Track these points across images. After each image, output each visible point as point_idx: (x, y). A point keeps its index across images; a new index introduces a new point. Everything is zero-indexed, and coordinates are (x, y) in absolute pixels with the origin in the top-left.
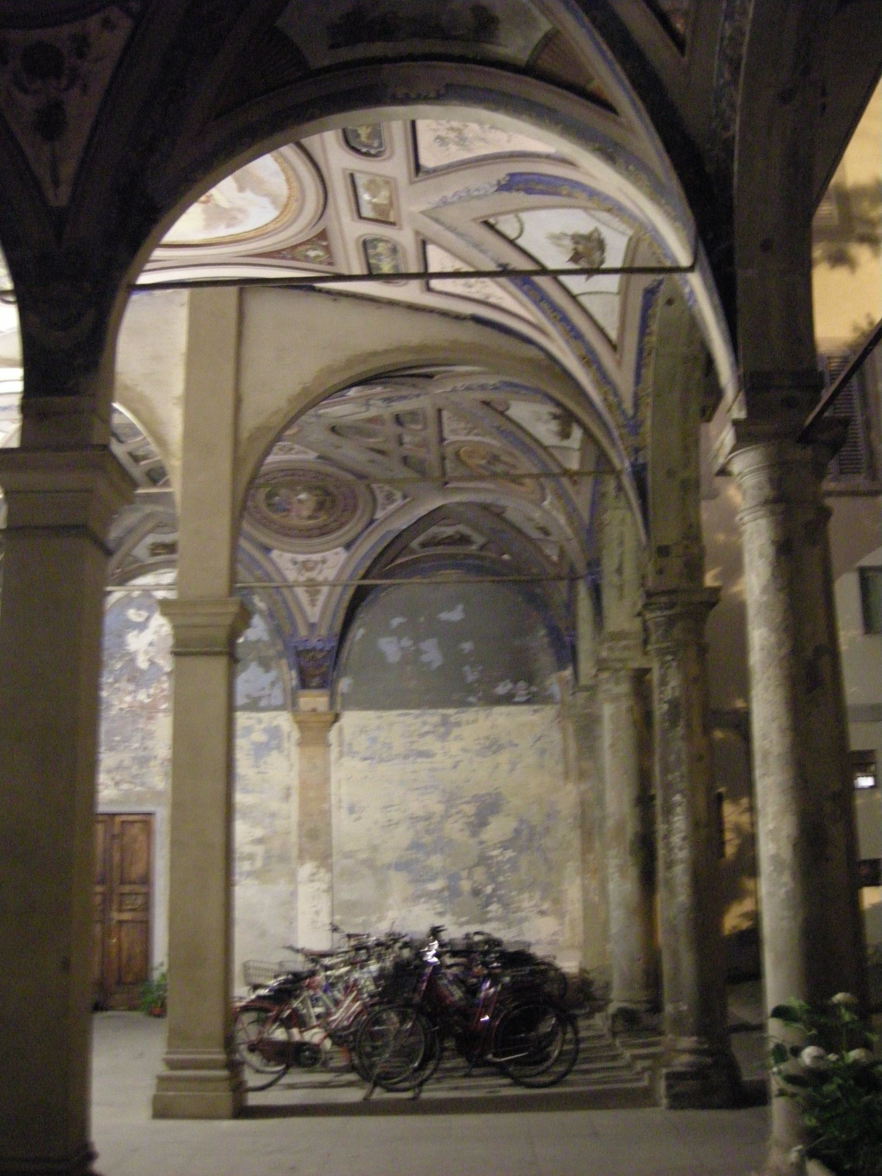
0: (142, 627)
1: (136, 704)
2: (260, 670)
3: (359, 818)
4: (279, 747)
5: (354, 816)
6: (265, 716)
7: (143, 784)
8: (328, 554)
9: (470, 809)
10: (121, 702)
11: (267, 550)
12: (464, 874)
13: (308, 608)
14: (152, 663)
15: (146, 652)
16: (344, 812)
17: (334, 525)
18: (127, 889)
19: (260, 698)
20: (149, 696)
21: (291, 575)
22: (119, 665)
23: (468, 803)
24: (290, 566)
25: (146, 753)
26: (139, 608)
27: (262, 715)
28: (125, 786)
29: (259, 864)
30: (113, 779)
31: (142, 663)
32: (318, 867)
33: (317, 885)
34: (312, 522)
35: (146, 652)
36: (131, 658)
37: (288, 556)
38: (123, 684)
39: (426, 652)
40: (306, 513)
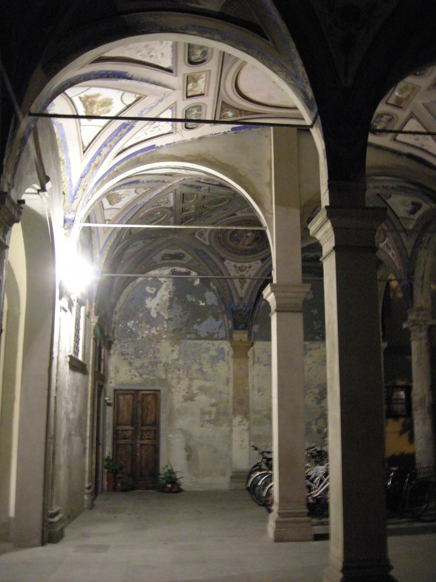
0: (154, 296)
1: (151, 335)
2: (214, 320)
3: (263, 395)
4: (223, 359)
5: (260, 394)
6: (217, 343)
7: (154, 375)
8: (253, 264)
9: (316, 391)
10: (143, 333)
11: (223, 260)
12: (314, 422)
13: (239, 290)
14: (158, 313)
15: (155, 309)
16: (256, 391)
18: (145, 428)
19: (214, 334)
20: (157, 331)
21: (233, 273)
22: (141, 315)
23: (316, 388)
24: (233, 268)
25: (156, 360)
26: (151, 286)
27: (215, 342)
28: (145, 376)
29: (213, 416)
30: (138, 373)
31: (154, 314)
32: (243, 418)
33: (242, 427)
34: (248, 247)
35: (155, 309)
36: (149, 312)
37: (232, 263)
38: (143, 325)
40: (247, 243)
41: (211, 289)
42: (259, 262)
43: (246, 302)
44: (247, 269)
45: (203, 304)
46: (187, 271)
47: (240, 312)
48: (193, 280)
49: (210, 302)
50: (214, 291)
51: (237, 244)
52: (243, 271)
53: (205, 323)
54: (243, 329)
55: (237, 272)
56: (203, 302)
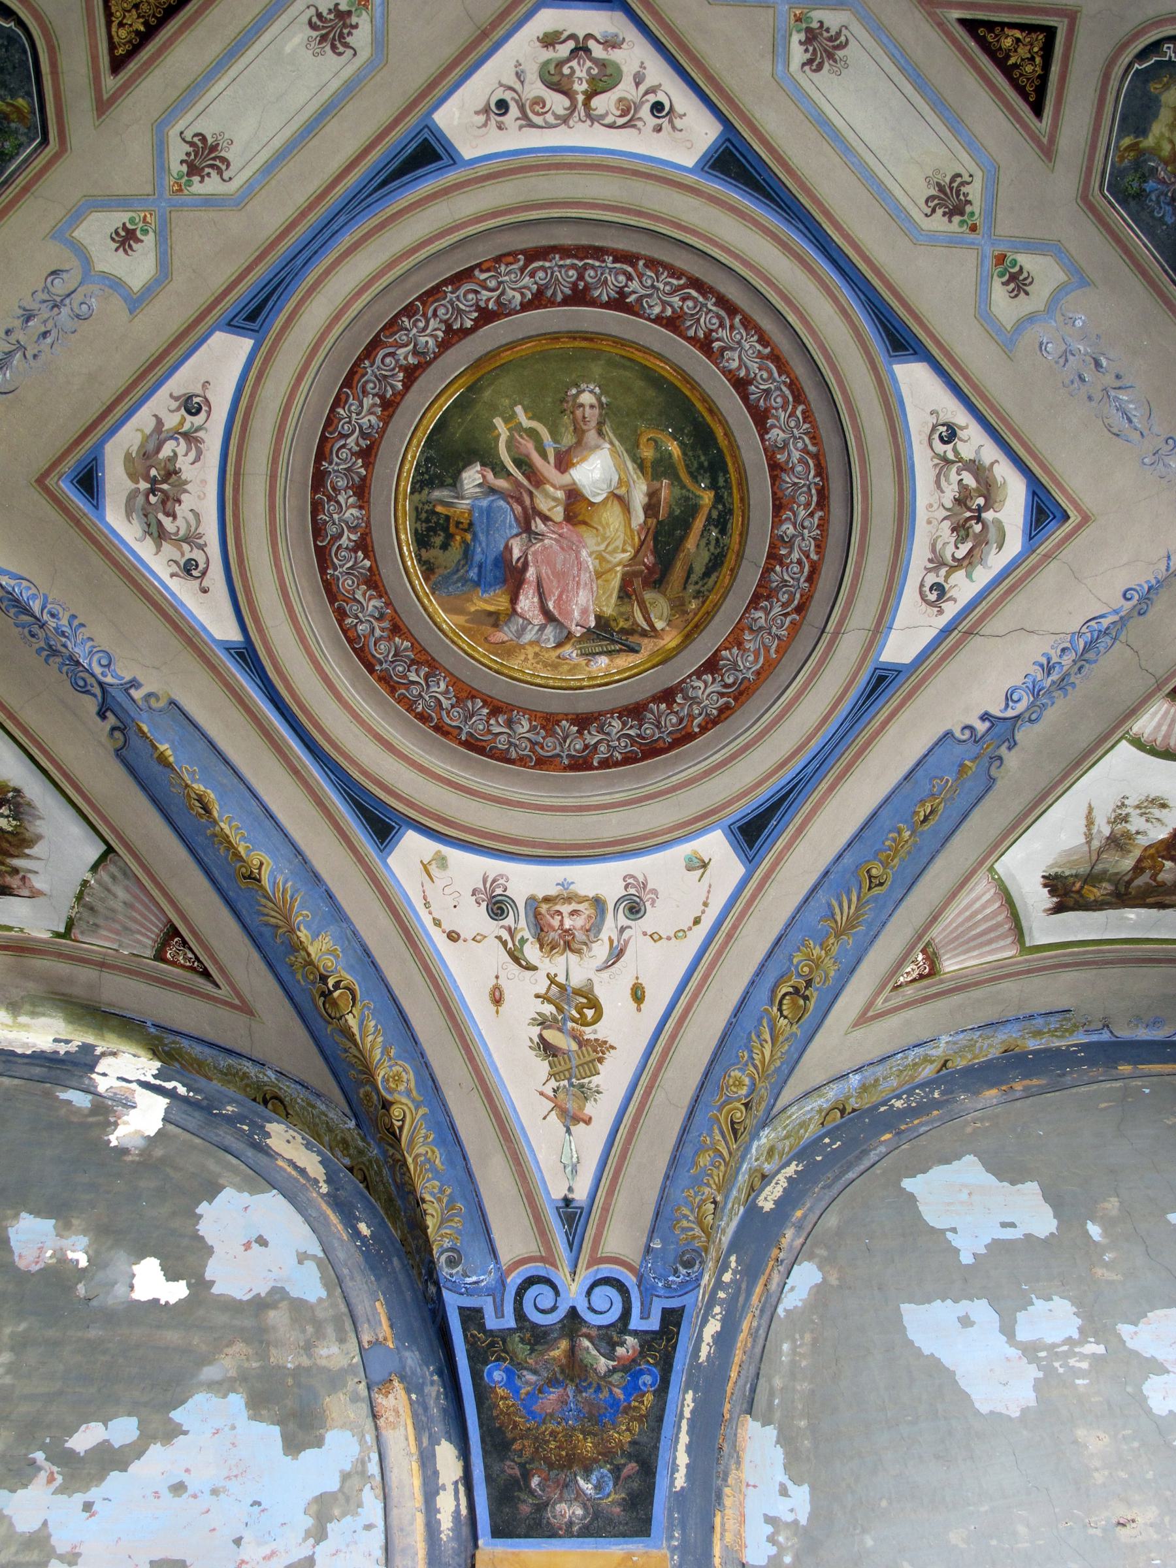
2: (267, 1436)
8: (660, 868)
17: (707, 692)
24: (474, 919)
37: (469, 868)
39: (1157, 1368)
41: (263, 1174)
42: (715, 844)
43: (622, 1238)
44: (609, 929)
45: (177, 1292)
46: (62, 1049)
47: (559, 1350)
48: (106, 1110)
49: (234, 1276)
50: (293, 1192)
51: (495, 619)
52: (569, 943)
53: (158, 1462)
54: (597, 1526)
55: (516, 957)
56: (171, 1275)
